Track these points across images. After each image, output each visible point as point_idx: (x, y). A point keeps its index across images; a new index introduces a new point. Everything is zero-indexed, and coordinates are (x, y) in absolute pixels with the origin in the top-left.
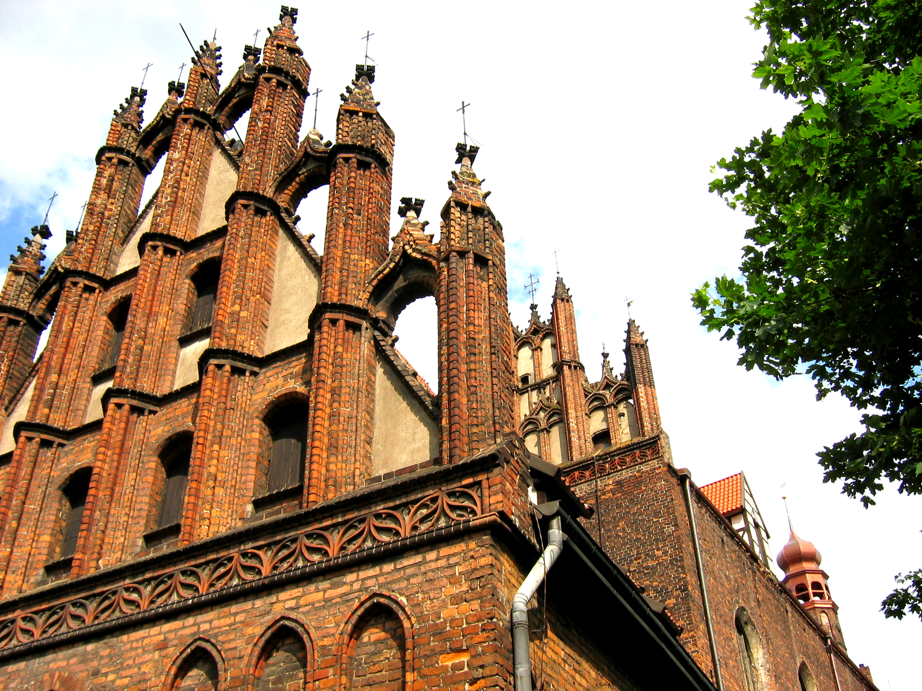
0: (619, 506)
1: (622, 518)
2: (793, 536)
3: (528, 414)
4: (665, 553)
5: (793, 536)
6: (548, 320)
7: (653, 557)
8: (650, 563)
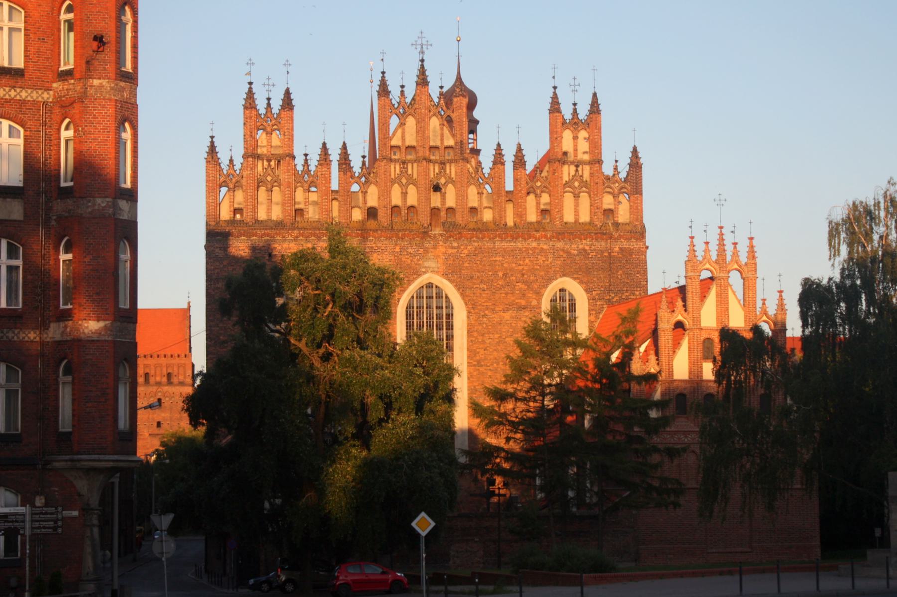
0: (621, 262)
1: (621, 269)
2: (459, 79)
3: (567, 180)
4: (640, 294)
5: (459, 79)
7: (634, 294)
8: (632, 297)
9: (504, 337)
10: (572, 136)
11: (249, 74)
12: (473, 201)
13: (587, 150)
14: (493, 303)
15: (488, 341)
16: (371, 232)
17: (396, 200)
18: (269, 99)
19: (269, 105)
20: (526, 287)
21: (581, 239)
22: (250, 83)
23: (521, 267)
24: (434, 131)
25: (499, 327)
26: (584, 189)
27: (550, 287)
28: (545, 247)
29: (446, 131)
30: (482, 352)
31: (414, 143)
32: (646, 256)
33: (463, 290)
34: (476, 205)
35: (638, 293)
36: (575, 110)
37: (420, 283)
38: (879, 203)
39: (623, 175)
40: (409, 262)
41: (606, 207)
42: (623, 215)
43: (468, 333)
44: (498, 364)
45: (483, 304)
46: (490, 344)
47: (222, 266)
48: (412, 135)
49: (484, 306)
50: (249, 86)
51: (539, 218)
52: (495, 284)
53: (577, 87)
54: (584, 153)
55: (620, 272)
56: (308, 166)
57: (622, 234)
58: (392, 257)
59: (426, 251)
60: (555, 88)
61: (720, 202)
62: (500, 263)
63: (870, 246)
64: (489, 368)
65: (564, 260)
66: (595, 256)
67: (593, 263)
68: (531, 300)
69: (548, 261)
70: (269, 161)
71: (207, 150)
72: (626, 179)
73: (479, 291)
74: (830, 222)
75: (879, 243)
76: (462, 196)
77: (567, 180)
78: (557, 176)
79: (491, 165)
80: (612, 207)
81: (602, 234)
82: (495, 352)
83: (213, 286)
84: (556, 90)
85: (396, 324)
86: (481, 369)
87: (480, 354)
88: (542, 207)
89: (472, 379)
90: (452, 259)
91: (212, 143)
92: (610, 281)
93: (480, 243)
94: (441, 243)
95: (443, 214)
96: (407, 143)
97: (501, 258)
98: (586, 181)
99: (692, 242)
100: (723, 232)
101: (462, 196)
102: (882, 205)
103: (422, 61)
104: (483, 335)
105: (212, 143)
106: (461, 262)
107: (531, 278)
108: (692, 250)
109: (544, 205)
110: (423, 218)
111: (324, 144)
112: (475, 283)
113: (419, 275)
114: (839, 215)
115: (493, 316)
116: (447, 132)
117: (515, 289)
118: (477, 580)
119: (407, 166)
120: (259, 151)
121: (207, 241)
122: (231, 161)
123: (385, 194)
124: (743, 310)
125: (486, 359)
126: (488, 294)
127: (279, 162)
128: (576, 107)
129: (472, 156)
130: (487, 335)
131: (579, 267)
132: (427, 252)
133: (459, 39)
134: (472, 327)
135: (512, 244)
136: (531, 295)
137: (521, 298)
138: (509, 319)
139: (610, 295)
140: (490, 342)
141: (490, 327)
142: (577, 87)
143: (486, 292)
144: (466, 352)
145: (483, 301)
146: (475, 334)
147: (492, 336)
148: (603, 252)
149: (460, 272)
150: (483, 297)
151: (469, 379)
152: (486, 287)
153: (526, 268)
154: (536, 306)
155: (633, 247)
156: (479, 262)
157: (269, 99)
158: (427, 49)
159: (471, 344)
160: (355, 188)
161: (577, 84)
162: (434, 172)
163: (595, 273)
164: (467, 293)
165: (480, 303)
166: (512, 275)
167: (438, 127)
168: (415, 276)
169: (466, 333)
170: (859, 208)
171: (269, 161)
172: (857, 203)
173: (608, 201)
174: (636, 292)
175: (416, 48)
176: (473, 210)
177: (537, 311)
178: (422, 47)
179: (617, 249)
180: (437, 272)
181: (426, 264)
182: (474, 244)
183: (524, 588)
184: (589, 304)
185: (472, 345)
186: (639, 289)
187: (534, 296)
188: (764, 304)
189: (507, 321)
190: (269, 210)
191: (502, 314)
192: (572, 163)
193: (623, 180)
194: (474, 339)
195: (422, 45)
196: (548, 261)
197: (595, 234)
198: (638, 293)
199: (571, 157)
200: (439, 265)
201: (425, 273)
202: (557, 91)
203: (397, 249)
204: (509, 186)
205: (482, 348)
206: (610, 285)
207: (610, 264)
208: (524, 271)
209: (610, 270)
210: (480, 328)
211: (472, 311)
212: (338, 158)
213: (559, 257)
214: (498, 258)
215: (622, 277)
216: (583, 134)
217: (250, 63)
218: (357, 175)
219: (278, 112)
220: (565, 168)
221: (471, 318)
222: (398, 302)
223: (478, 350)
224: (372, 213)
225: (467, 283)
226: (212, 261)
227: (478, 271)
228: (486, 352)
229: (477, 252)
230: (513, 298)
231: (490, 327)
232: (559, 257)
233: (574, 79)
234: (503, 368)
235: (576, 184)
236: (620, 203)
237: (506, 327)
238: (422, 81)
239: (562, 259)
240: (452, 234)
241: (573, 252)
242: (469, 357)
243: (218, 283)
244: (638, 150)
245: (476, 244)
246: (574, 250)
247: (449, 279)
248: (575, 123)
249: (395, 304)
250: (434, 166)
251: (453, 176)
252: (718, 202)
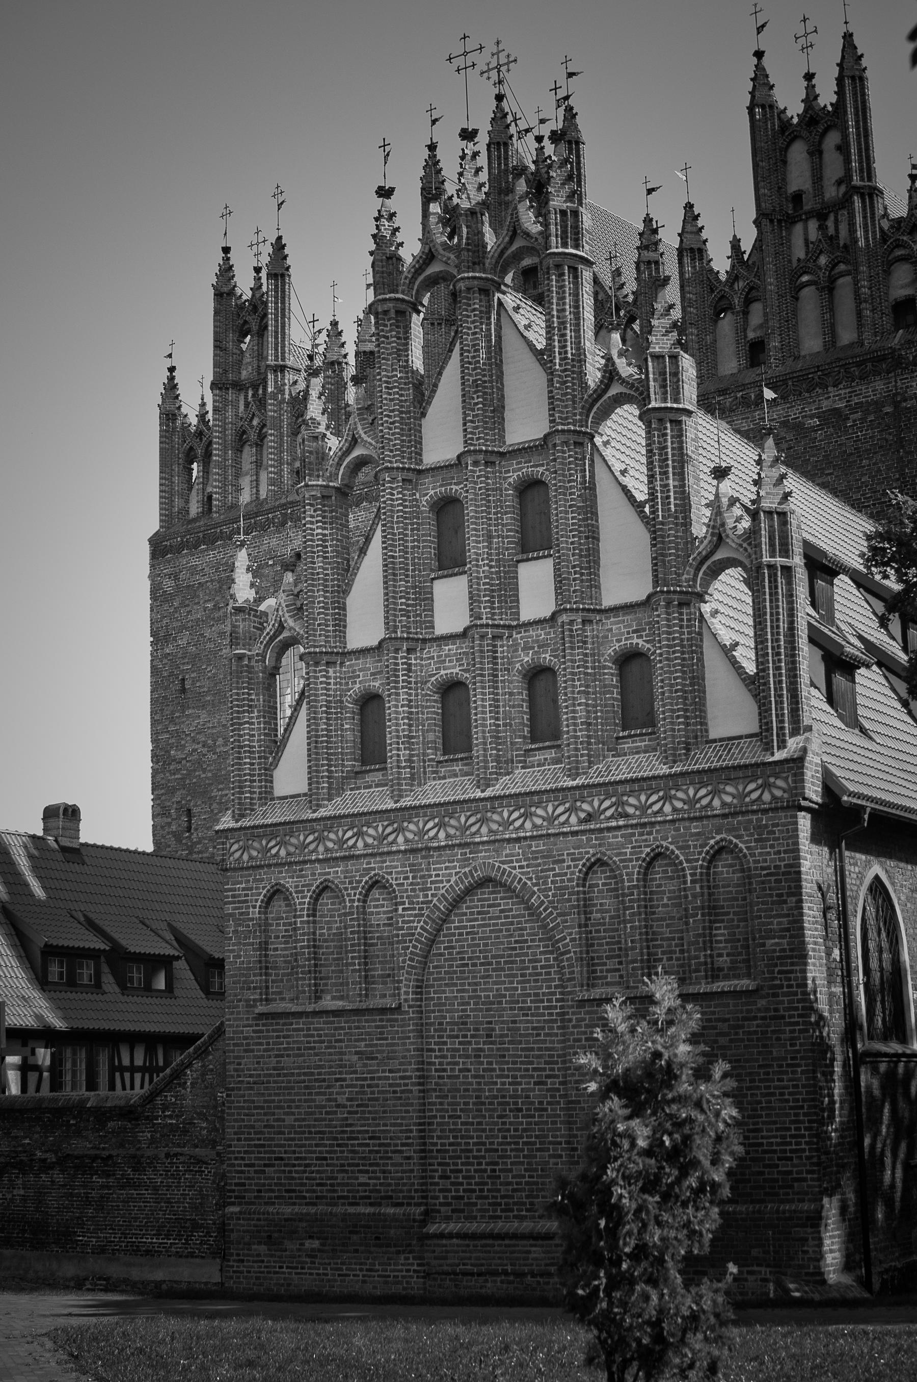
3: (802, 255)
6: (832, 104)
26: (842, 267)
36: (810, 88)
60: (759, 54)
66: (863, 420)
88: (751, 335)
121: (152, 566)
128: (814, 82)
148: (878, 405)
192: (810, 215)
197: (858, 364)
220: (798, 228)
233: (805, 20)
246: (812, 417)
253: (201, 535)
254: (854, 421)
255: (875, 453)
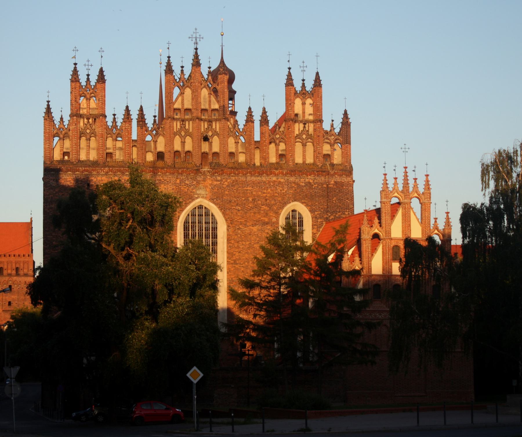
1: (335, 196)
2: (222, 61)
3: (298, 133)
4: (349, 214)
5: (222, 61)
7: (344, 214)
8: (343, 216)
9: (253, 244)
10: (301, 102)
11: (74, 57)
12: (232, 148)
13: (312, 113)
14: (245, 220)
15: (241, 247)
16: (160, 170)
17: (177, 146)
18: (88, 75)
19: (88, 79)
20: (268, 209)
21: (307, 175)
22: (75, 64)
23: (265, 195)
24: (204, 99)
25: (249, 237)
26: (309, 140)
27: (285, 208)
28: (282, 180)
29: (213, 99)
30: (237, 254)
31: (190, 107)
32: (353, 187)
33: (224, 211)
34: (233, 150)
35: (347, 213)
36: (303, 84)
37: (194, 205)
38: (517, 151)
39: (337, 130)
40: (186, 190)
41: (325, 152)
42: (337, 158)
43: (227, 240)
44: (248, 263)
45: (238, 220)
46: (242, 248)
47: (54, 192)
48: (189, 101)
49: (238, 222)
50: (74, 66)
51: (278, 160)
52: (247, 206)
53: (305, 68)
54: (310, 114)
55: (335, 198)
56: (116, 123)
57: (336, 172)
58: (174, 187)
59: (198, 183)
60: (290, 68)
61: (405, 150)
62: (250, 192)
63: (510, 181)
64: (242, 265)
65: (295, 190)
67: (315, 192)
68: (272, 218)
69: (284, 190)
70: (88, 119)
71: (45, 111)
72: (339, 133)
73: (235, 211)
74: (483, 164)
75: (516, 179)
76: (224, 144)
77: (298, 133)
78: (291, 130)
79: (244, 123)
80: (329, 153)
81: (322, 171)
82: (246, 254)
83: (48, 207)
84: (291, 70)
85: (177, 234)
86: (237, 266)
87: (236, 255)
88: (280, 152)
89: (230, 273)
90: (217, 188)
91: (48, 106)
92: (327, 205)
93: (236, 178)
94: (209, 177)
95: (210, 157)
96: (186, 107)
97: (251, 188)
98: (311, 135)
99: (385, 178)
100: (407, 171)
101: (224, 144)
102: (519, 153)
103: (196, 49)
104: (238, 242)
105: (48, 106)
106: (223, 191)
107: (272, 202)
108: (385, 184)
109: (283, 150)
110: (197, 160)
111: (127, 107)
112: (232, 206)
113: (193, 200)
114: (489, 159)
115: (245, 229)
116: (214, 99)
117: (260, 210)
118: (233, 415)
119: (185, 123)
120: (81, 112)
122: (62, 119)
123: (170, 142)
124: (421, 226)
125: (240, 259)
126: (241, 213)
127: (95, 119)
128: (305, 82)
129: (231, 116)
130: (240, 243)
131: (306, 195)
132: (199, 184)
133: (222, 34)
134: (230, 237)
135: (259, 178)
136: (272, 214)
137: (265, 217)
138: (256, 231)
139: (327, 215)
140: (243, 247)
141: (243, 237)
142: (305, 68)
143: (240, 212)
144: (226, 254)
145: (238, 219)
146: (233, 242)
147: (244, 243)
148: (322, 184)
149: (222, 198)
150: (238, 216)
151: (228, 273)
152: (240, 209)
153: (268, 195)
154: (275, 222)
155: (344, 181)
156: (235, 191)
157: (88, 75)
158: (200, 41)
159: (229, 248)
160: (149, 138)
161: (305, 66)
162: (204, 127)
163: (317, 199)
164: (227, 213)
165: (236, 220)
166: (259, 200)
167: (207, 96)
168: (190, 200)
169: (226, 240)
170: (503, 154)
171: (88, 119)
172: (502, 151)
173: (326, 149)
174: (346, 213)
175: (192, 40)
176: (232, 154)
177: (276, 225)
178: (196, 40)
179: (332, 182)
180: (206, 198)
181: (198, 192)
182: (232, 178)
183: (266, 421)
184: (312, 221)
185: (230, 249)
186: (348, 211)
187: (274, 215)
188: (436, 222)
189: (255, 232)
190: (88, 154)
191: (251, 227)
192: (301, 122)
193: (337, 134)
194: (232, 245)
195: (196, 38)
196: (284, 190)
197: (317, 171)
198: (347, 213)
199: (300, 118)
200: (207, 193)
201: (197, 198)
202: (291, 71)
203: (178, 181)
204: (257, 137)
205: (237, 252)
206: (328, 208)
207: (328, 193)
208: (267, 198)
209: (328, 197)
210: (236, 237)
211: (230, 225)
212: (137, 117)
213: (292, 187)
214: (249, 188)
215: (336, 202)
216: (309, 101)
217: (76, 50)
218: (150, 129)
219: (94, 84)
220: (297, 125)
221: (230, 230)
222: (179, 218)
223: (234, 253)
224: (160, 156)
225: (227, 205)
226: (48, 188)
227: (235, 197)
228: (240, 254)
229: (234, 184)
230: (259, 216)
231: (243, 237)
232: (292, 187)
233: (303, 62)
234: (251, 265)
235: (304, 136)
236: (335, 150)
237: (254, 237)
238: (196, 63)
239: (294, 189)
240: (217, 171)
241: (301, 184)
242: (228, 258)
243: (52, 204)
244: (348, 113)
245: (233, 178)
246: (302, 183)
247: (214, 203)
248: (303, 94)
249: (176, 220)
250: (204, 123)
251: (218, 130)
252: (404, 150)
253: (69, 168)
254: (315, 187)
255: (320, 197)
